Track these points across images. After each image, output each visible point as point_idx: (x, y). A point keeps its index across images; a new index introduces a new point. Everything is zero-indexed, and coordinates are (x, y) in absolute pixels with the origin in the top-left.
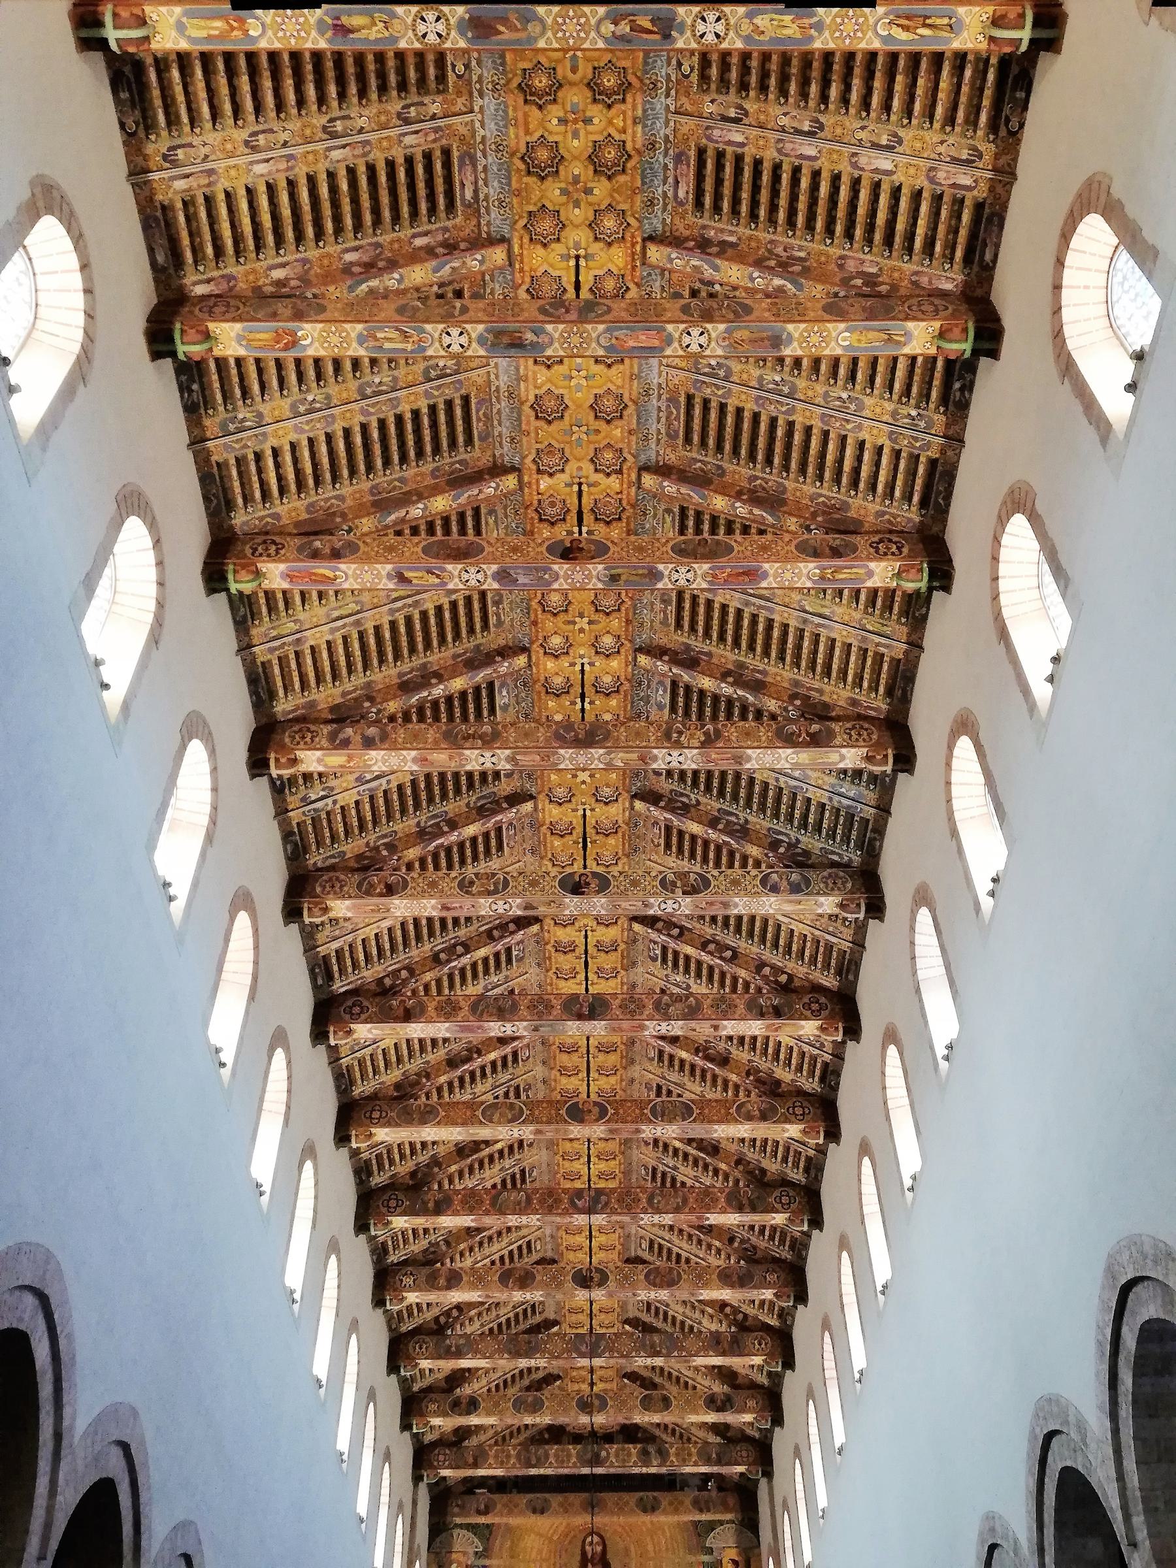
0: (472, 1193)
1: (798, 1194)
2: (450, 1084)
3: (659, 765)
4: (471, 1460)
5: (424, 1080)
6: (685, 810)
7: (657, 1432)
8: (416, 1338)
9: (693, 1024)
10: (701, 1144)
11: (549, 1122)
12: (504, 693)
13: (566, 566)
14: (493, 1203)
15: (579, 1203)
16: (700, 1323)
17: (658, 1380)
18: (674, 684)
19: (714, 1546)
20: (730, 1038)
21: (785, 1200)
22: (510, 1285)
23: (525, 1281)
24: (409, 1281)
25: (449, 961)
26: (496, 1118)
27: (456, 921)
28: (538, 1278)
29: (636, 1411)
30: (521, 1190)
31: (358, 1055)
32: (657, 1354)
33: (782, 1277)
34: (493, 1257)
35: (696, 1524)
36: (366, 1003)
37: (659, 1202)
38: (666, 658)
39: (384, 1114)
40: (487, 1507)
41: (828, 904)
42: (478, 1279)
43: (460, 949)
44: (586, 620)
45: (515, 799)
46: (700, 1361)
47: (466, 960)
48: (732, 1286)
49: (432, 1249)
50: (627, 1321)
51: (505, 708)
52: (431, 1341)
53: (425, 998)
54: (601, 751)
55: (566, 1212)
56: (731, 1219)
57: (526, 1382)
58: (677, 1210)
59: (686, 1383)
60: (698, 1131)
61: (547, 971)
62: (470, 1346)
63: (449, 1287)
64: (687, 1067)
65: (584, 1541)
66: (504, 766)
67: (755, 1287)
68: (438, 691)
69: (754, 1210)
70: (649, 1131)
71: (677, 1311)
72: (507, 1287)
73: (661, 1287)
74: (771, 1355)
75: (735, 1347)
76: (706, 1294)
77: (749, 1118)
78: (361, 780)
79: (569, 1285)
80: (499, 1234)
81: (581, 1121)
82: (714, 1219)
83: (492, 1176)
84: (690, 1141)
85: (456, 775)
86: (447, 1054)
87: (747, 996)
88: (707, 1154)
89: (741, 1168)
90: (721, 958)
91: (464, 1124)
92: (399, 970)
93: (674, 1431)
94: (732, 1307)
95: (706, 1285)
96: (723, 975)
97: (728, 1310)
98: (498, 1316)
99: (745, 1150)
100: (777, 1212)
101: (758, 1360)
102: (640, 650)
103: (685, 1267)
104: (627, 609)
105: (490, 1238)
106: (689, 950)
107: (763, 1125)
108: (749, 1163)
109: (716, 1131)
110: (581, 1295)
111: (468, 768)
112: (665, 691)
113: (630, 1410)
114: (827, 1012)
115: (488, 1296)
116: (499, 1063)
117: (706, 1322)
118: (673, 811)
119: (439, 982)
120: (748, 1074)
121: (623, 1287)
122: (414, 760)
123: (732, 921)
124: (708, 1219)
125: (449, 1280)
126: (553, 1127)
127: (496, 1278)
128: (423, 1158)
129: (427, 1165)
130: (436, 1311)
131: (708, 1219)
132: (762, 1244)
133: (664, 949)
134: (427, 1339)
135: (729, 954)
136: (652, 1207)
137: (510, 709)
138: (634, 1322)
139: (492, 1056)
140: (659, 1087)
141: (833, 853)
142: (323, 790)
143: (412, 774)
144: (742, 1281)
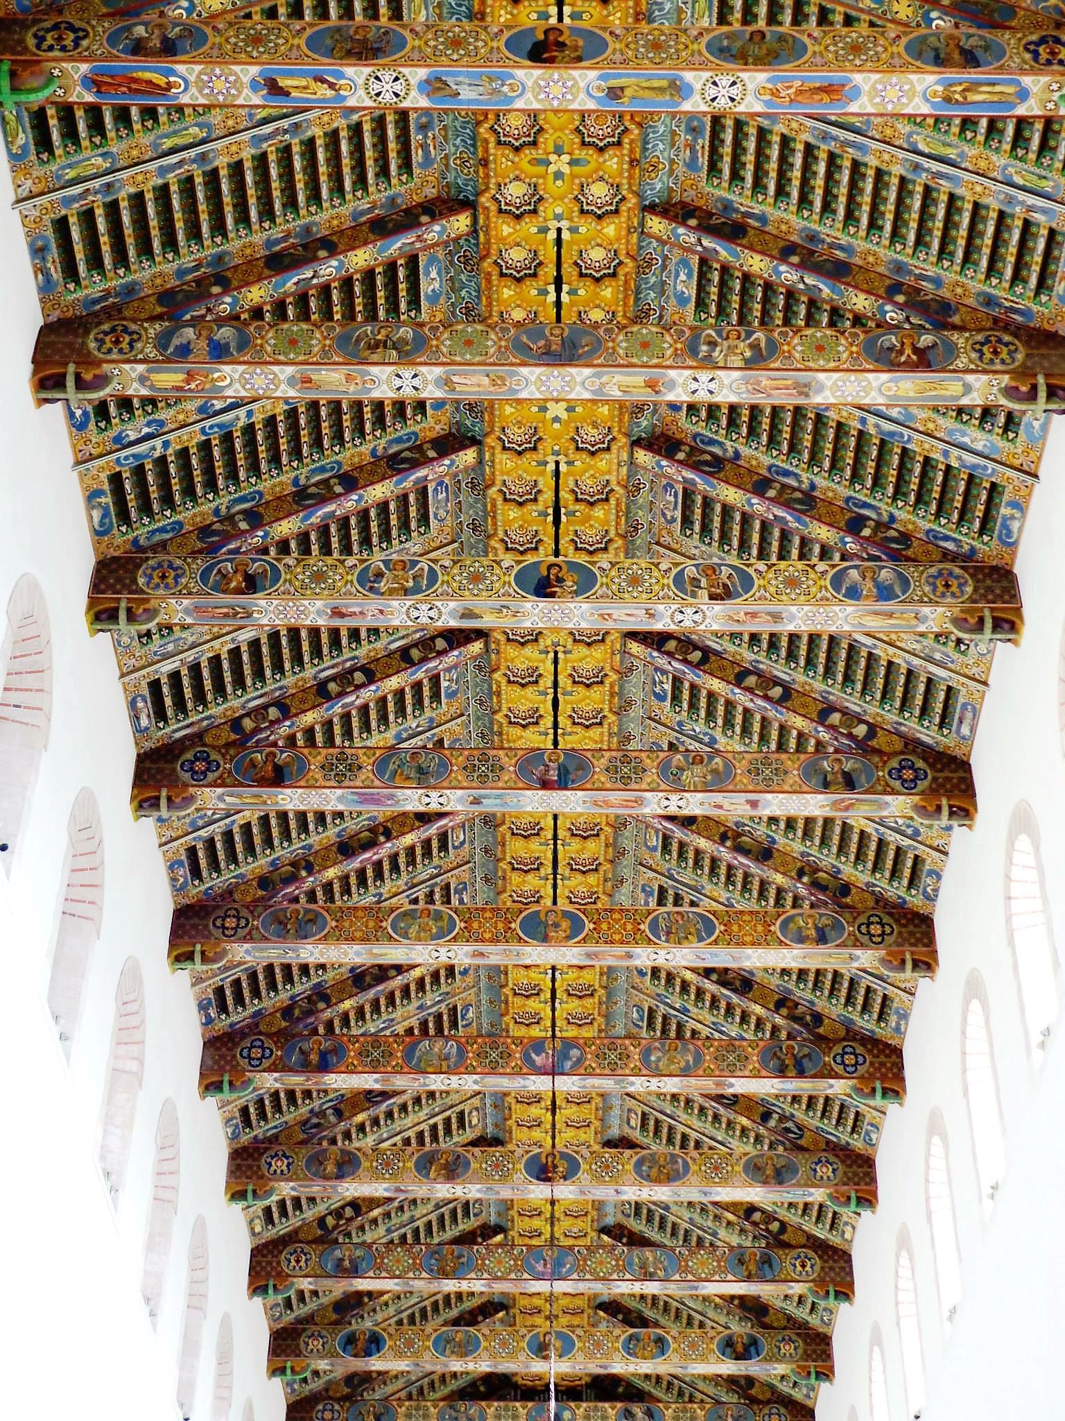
0: (376, 1039)
1: (870, 1051)
2: (345, 879)
3: (679, 395)
5: (304, 873)
6: (716, 466)
7: (647, 1387)
8: (290, 1249)
9: (718, 798)
10: (723, 977)
11: (494, 940)
12: (434, 274)
13: (537, 73)
14: (409, 1053)
15: (539, 1060)
16: (714, 1234)
17: (649, 1313)
20: (773, 820)
21: (850, 1059)
22: (432, 1175)
23: (453, 1170)
24: (280, 1165)
25: (342, 694)
26: (413, 931)
27: (354, 634)
28: (474, 1165)
29: (617, 1357)
30: (448, 1039)
31: (203, 833)
32: (649, 1277)
33: (840, 1173)
34: (411, 1133)
36: (214, 756)
37: (659, 1059)
38: (693, 222)
39: (243, 923)
41: (936, 617)
42: (386, 1165)
43: (359, 677)
44: (566, 158)
45: (448, 444)
46: (711, 1289)
47: (368, 694)
48: (765, 1183)
49: (315, 1120)
50: (605, 1230)
51: (433, 299)
52: (313, 1252)
54: (587, 371)
55: (518, 1073)
56: (766, 1087)
57: (454, 1313)
58: (685, 1072)
59: (690, 1317)
60: (722, 957)
62: (374, 1261)
63: (340, 1176)
64: (707, 863)
66: (432, 392)
67: (798, 1185)
68: (329, 269)
69: (801, 1074)
70: (644, 957)
71: (682, 1218)
72: (427, 1176)
73: (658, 1181)
74: (820, 1282)
75: (763, 1268)
76: (725, 1194)
77: (801, 939)
78: (206, 412)
79: (521, 1175)
80: (417, 1101)
81: (545, 939)
82: (740, 1086)
83: (406, 1016)
84: (707, 972)
86: (339, 835)
87: (803, 757)
88: (735, 991)
89: (784, 1011)
90: (766, 698)
91: (365, 940)
92: (265, 707)
93: (670, 1384)
94: (763, 1212)
95: (725, 1181)
97: (757, 1216)
98: (412, 1219)
99: (791, 986)
100: (837, 1076)
101: (797, 1289)
102: (651, 209)
103: (695, 1154)
104: (632, 141)
105: (404, 1108)
106: (716, 685)
107: (822, 949)
108: (797, 1004)
109: (749, 957)
110: (539, 1192)
111: (376, 394)
112: (689, 275)
113: (607, 1355)
114: (926, 783)
115: (398, 1190)
116: (418, 851)
117: (723, 1233)
118: (696, 467)
119: (328, 725)
120: (801, 873)
121: (599, 1179)
122: (291, 382)
123: (784, 643)
124: (731, 1085)
125: (340, 1165)
126: (500, 947)
127: (410, 1165)
128: (301, 987)
129: (309, 998)
130: (321, 1209)
131: (731, 1085)
132: (813, 1121)
133: (677, 681)
134: (307, 1248)
135: (777, 692)
136: (648, 1066)
138: (617, 1232)
139: (408, 839)
140: (662, 890)
141: (946, 538)
142: (148, 424)
143: (287, 403)
144: (779, 1176)
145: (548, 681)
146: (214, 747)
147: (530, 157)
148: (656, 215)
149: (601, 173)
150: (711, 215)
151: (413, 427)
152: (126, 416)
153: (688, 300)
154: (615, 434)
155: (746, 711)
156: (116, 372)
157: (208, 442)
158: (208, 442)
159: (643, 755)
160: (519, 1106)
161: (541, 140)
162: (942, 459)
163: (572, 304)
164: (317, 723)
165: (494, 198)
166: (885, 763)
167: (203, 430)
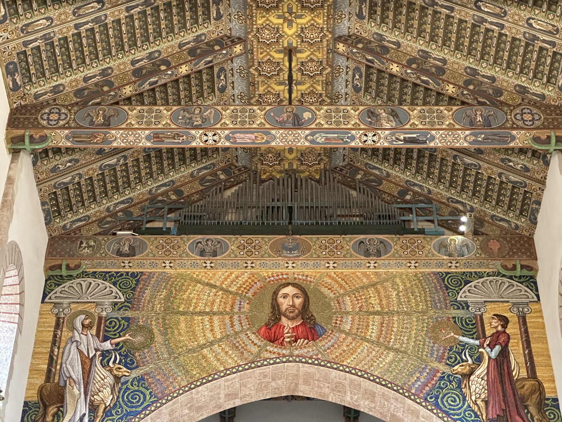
4: (101, 119)
40: (132, 248)
61: (253, 157)
65: (275, 294)
102: (339, 39)
104: (328, 6)
111: (194, 144)
122: (148, 138)
142: (70, 161)
146: (63, 106)
148: (341, 42)
149: (312, 22)
150: (370, 42)
156: (53, 134)
159: (349, 108)
162: (498, 178)
165: (256, 69)
166: (511, 111)
167: (100, 168)
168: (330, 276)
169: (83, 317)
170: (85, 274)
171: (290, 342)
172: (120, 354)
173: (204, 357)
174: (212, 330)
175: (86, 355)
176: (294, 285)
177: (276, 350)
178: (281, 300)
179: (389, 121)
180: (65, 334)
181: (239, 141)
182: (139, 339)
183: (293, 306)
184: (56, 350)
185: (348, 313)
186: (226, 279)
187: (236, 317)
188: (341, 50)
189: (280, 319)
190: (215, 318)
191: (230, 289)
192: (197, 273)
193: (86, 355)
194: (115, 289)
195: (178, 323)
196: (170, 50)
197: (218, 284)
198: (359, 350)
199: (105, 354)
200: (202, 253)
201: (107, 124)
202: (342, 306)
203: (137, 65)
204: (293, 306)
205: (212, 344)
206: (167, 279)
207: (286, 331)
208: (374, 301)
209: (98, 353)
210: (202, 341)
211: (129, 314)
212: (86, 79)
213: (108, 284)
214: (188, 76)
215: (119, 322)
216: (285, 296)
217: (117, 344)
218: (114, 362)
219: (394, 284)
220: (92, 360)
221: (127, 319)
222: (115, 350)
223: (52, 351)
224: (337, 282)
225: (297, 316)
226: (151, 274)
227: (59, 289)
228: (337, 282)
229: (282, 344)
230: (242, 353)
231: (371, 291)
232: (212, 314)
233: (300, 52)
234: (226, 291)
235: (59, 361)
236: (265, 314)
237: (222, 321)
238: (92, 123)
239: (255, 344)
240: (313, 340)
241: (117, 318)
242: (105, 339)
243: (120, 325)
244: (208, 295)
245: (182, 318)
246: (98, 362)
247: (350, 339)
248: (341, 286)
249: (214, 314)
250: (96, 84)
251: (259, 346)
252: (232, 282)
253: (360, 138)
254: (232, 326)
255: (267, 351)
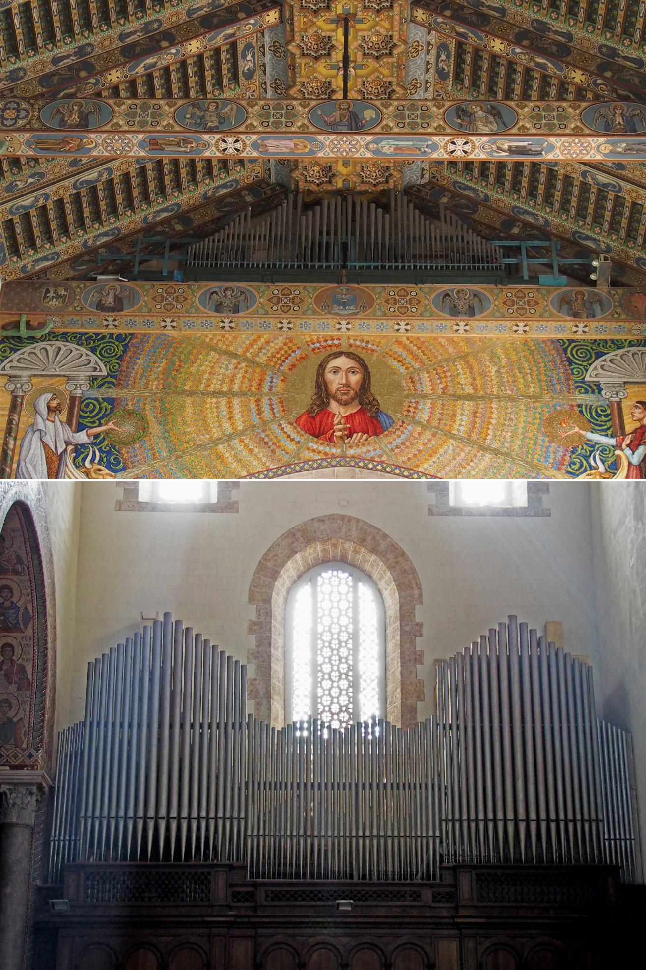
3: (440, 154)
4: (75, 118)
12: (249, 58)
18: (460, 45)
19: (602, 380)
35: (563, 346)
38: (448, 13)
40: (119, 300)
51: (249, 75)
53: (111, 102)
54: (369, 138)
65: (322, 367)
78: (77, 167)
85: (192, 163)
96: (532, 193)
111: (207, 154)
122: (141, 145)
137: (256, 77)
142: (32, 176)
143: (137, 161)
145: (338, 55)
146: (24, 99)
147: (324, 18)
148: (421, 8)
151: (235, 176)
152: (15, 170)
153: (447, 75)
154: (395, 41)
155: (527, 71)
156: (9, 139)
157: (78, 194)
158: (78, 194)
159: (429, 103)
160: (303, 61)
161: (333, 6)
163: (356, 76)
164: (121, 83)
165: (299, 46)
167: (74, 186)
168: (400, 343)
169: (49, 396)
170: (52, 336)
171: (341, 437)
172: (100, 450)
173: (220, 457)
174: (230, 418)
175: (53, 449)
176: (349, 355)
177: (321, 448)
178: (329, 376)
179: (487, 122)
180: (24, 420)
181: (271, 150)
182: (128, 429)
183: (348, 385)
184: (12, 442)
185: (425, 397)
186: (251, 345)
187: (265, 401)
188: (419, 19)
189: (329, 403)
190: (236, 401)
191: (257, 359)
192: (210, 335)
193: (53, 449)
194: (94, 358)
195: (183, 406)
196: (174, 19)
197: (240, 351)
198: (441, 451)
199: (79, 450)
200: (218, 308)
201: (84, 125)
202: (418, 386)
203: (128, 41)
204: (348, 385)
205: (230, 437)
206: (167, 344)
207: (336, 421)
208: (464, 379)
209: (70, 448)
210: (216, 433)
211: (113, 393)
212: (55, 61)
213: (83, 350)
214: (200, 57)
215: (100, 404)
216: (336, 370)
217: (96, 436)
218: (92, 461)
219: (493, 355)
220: (61, 457)
221: (111, 401)
222: (92, 444)
223: (6, 443)
224: (409, 351)
225: (353, 399)
226: (145, 338)
227: (15, 356)
228: (409, 351)
229: (330, 439)
230: (273, 451)
231: (460, 365)
232: (230, 394)
233: (361, 21)
234: (252, 362)
235: (16, 458)
236: (306, 397)
237: (245, 406)
238: (63, 123)
239: (292, 440)
240: (376, 434)
241: (96, 399)
242: (80, 428)
243: (101, 409)
244: (226, 367)
245: (189, 400)
246: (69, 459)
247: (428, 434)
248: (416, 358)
249: (235, 395)
250: (70, 68)
251: (298, 442)
252: (260, 349)
253: (445, 148)
254: (260, 412)
255: (308, 449)
